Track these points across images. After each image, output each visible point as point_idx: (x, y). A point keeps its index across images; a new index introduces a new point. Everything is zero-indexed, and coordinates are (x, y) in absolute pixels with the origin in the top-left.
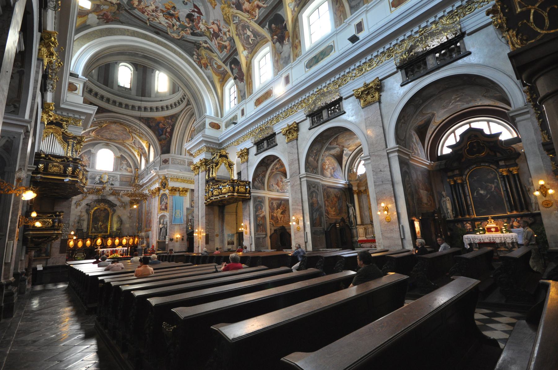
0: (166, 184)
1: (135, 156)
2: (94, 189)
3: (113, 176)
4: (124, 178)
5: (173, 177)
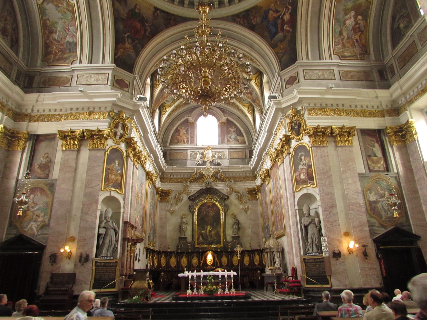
0: (300, 126)
1: (246, 116)
2: (196, 174)
3: (220, 152)
4: (236, 153)
5: (312, 105)
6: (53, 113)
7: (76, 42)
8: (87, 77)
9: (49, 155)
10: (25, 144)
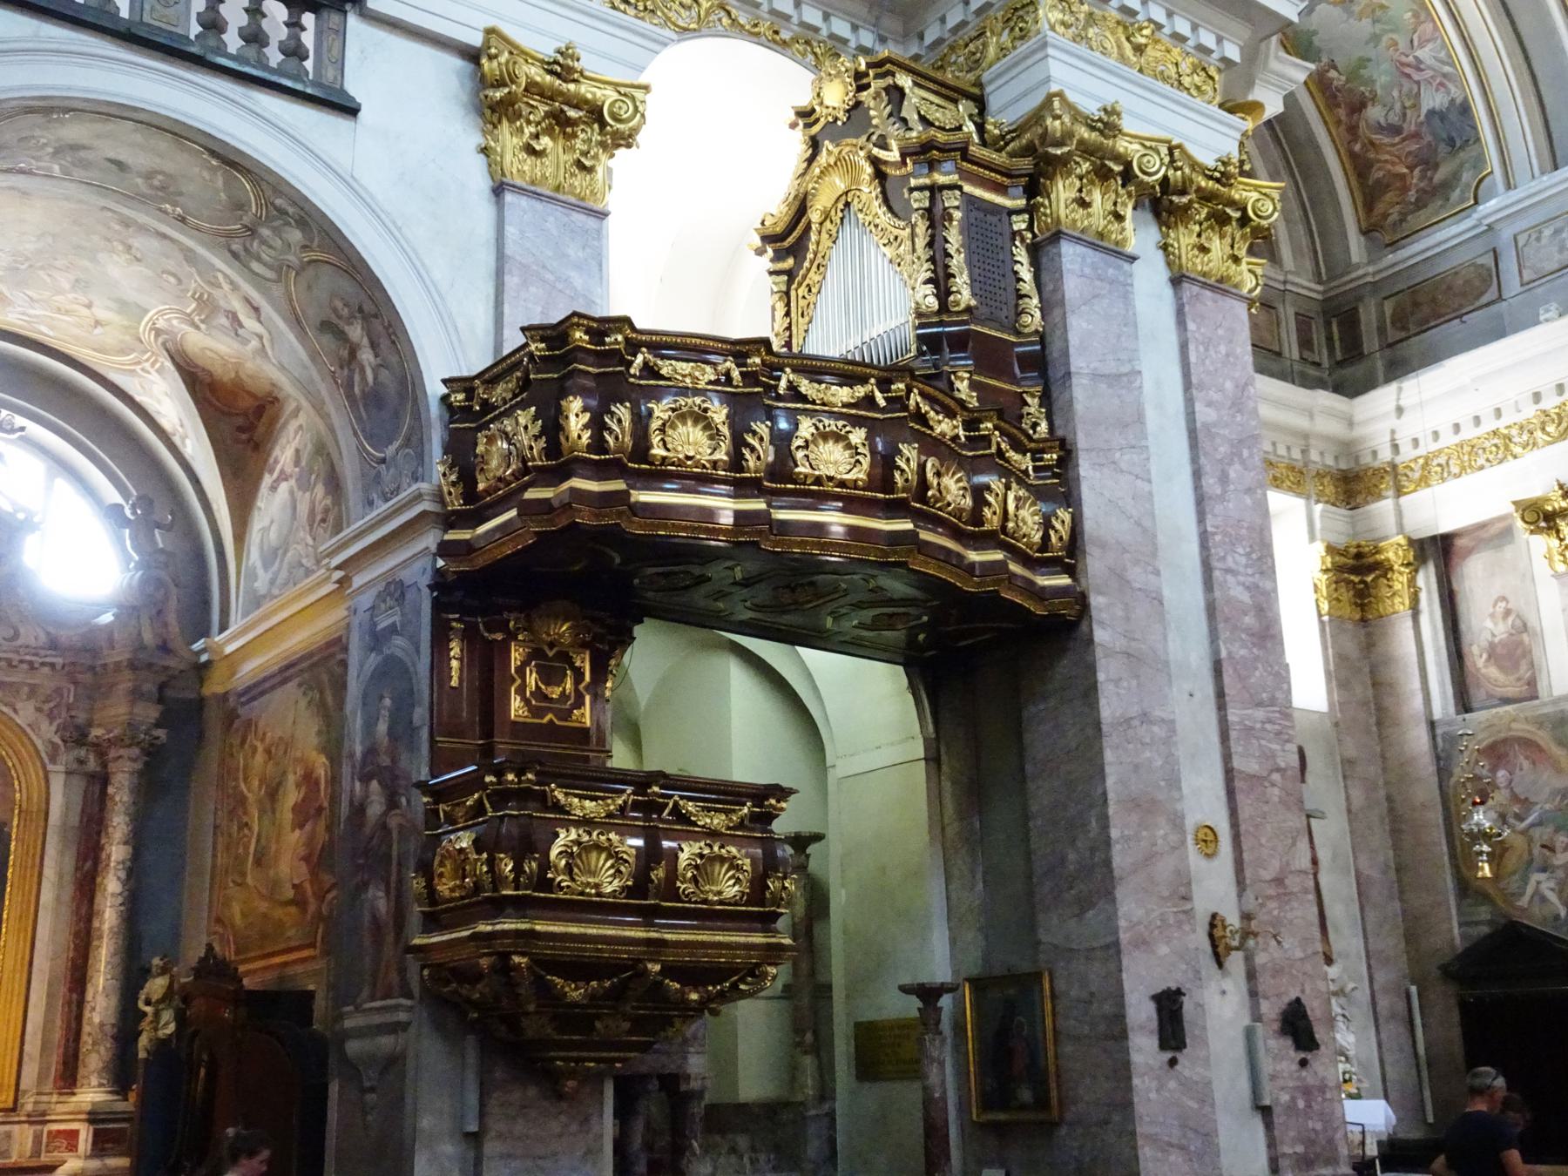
6: (1469, 433)
7: (1466, 99)
8: (1557, 232)
9: (1509, 606)
10: (1412, 582)
